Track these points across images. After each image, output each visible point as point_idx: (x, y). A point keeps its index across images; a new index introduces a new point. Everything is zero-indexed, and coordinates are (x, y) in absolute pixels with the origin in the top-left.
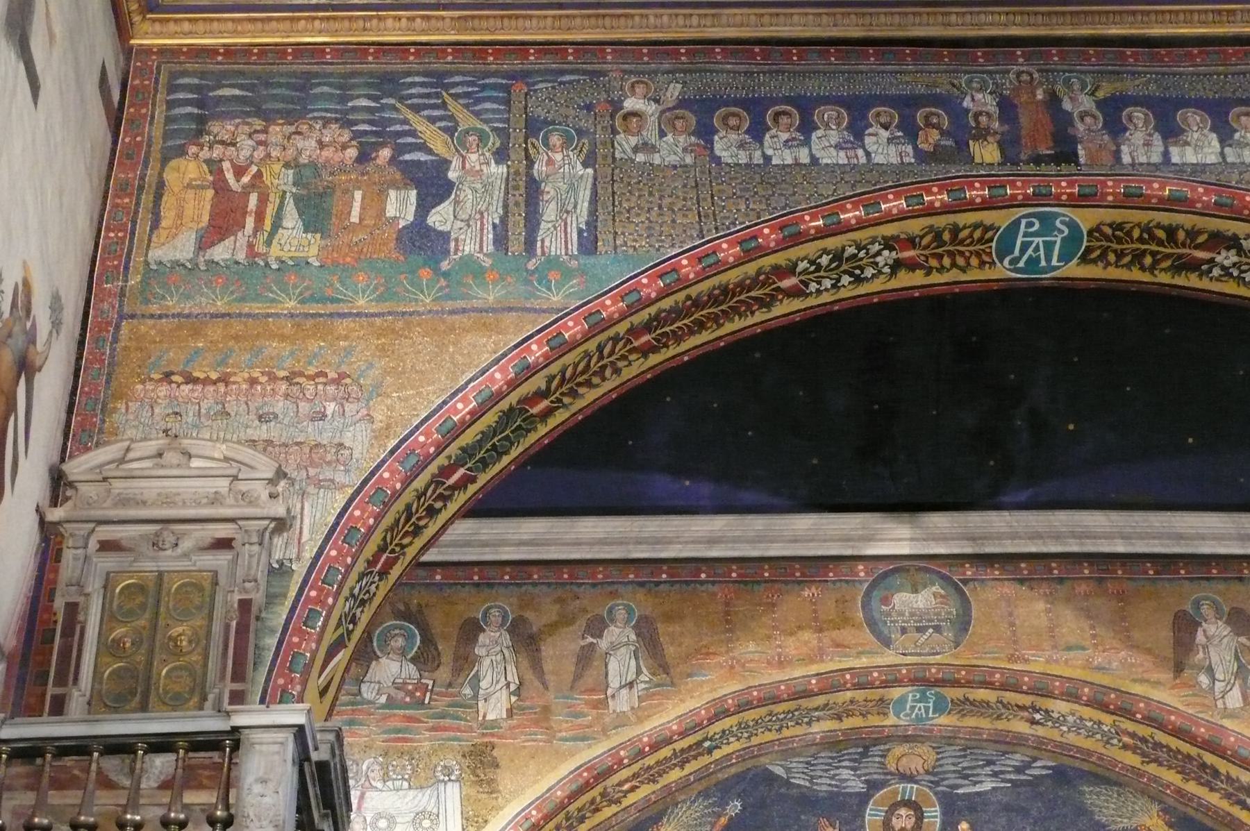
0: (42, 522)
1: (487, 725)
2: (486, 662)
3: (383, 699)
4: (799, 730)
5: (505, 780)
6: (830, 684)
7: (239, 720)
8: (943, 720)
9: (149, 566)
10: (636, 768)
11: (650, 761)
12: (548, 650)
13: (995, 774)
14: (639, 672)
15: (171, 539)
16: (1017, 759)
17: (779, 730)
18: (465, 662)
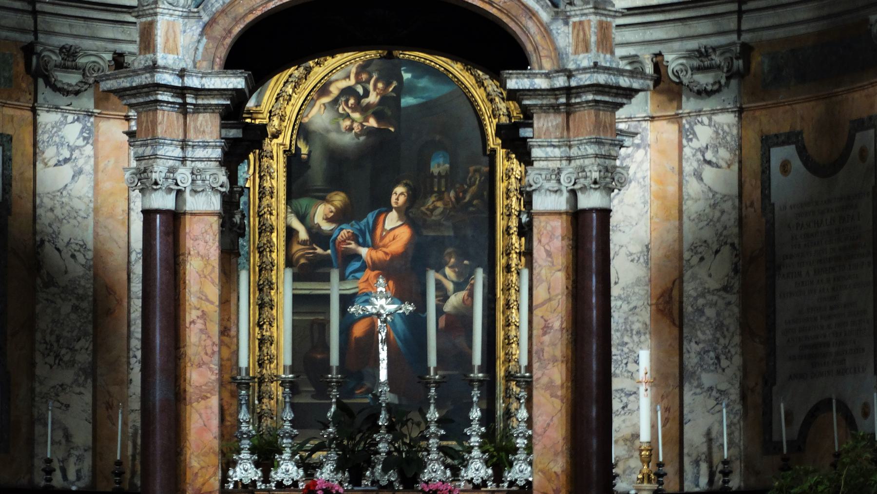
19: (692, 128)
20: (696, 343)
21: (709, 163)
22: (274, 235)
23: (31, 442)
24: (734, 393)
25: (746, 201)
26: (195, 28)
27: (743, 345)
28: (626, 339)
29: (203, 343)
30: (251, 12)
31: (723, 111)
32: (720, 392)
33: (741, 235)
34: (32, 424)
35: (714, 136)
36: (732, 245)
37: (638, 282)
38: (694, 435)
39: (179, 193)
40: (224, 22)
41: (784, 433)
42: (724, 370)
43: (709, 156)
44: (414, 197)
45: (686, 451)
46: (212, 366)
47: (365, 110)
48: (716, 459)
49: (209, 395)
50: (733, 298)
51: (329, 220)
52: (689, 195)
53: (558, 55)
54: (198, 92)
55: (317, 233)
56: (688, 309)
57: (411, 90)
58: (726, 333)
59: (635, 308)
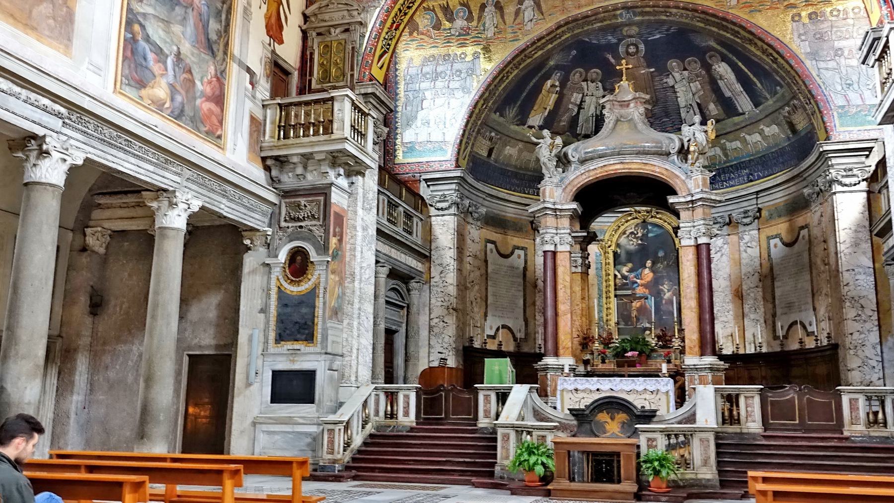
0: (302, 30)
1: (486, 38)
2: (487, 18)
3: (457, 34)
4: (590, 27)
5: (494, 57)
6: (595, 13)
7: (332, 95)
8: (637, 18)
9: (329, 39)
10: (534, 47)
11: (539, 44)
12: (506, 11)
13: (659, 32)
14: (534, 16)
15: (332, 30)
16: (665, 27)
17: (583, 28)
18: (480, 18)
23: (535, 339)
24: (762, 321)
25: (762, 258)
26: (560, 190)
27: (764, 305)
30: (579, 183)
31: (753, 230)
34: (535, 334)
38: (749, 335)
39: (556, 245)
40: (569, 188)
41: (780, 333)
43: (749, 245)
44: (654, 263)
47: (637, 238)
48: (757, 342)
50: (760, 290)
53: (689, 190)
54: (561, 210)
56: (744, 294)
57: (652, 232)
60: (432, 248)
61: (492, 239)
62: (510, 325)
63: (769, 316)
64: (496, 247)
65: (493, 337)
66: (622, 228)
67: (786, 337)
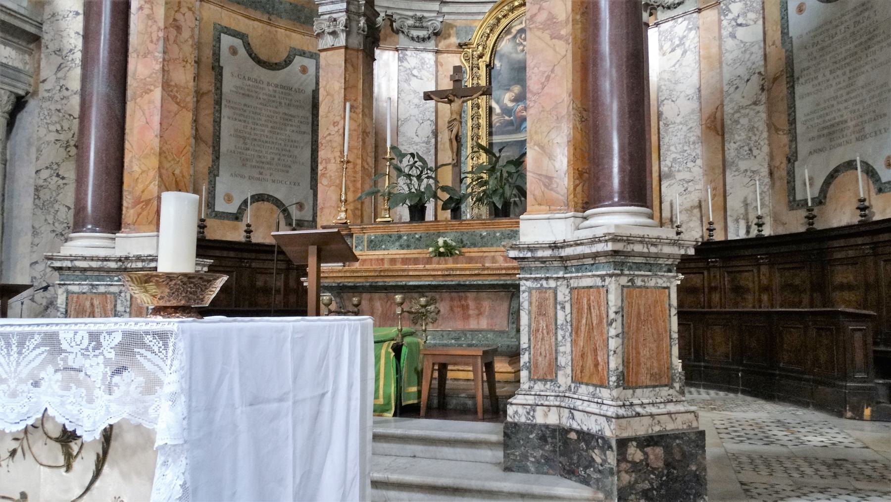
19: (727, 7)
20: (735, 143)
21: (740, 25)
22: (481, 109)
24: (765, 171)
25: (769, 42)
28: (686, 148)
29: (149, 30)
32: (753, 172)
33: (766, 66)
35: (744, 6)
36: (760, 73)
37: (693, 112)
38: (734, 203)
42: (755, 157)
43: (740, 21)
45: (728, 214)
46: (157, 54)
49: (152, 88)
50: (762, 108)
51: (512, 101)
52: (726, 50)
55: (505, 109)
56: (728, 122)
58: (756, 132)
59: (691, 128)
60: (46, 17)
61: (233, 26)
62: (278, 196)
63: (780, 161)
64: (247, 46)
65: (237, 217)
66: (504, 22)
67: (820, 200)
